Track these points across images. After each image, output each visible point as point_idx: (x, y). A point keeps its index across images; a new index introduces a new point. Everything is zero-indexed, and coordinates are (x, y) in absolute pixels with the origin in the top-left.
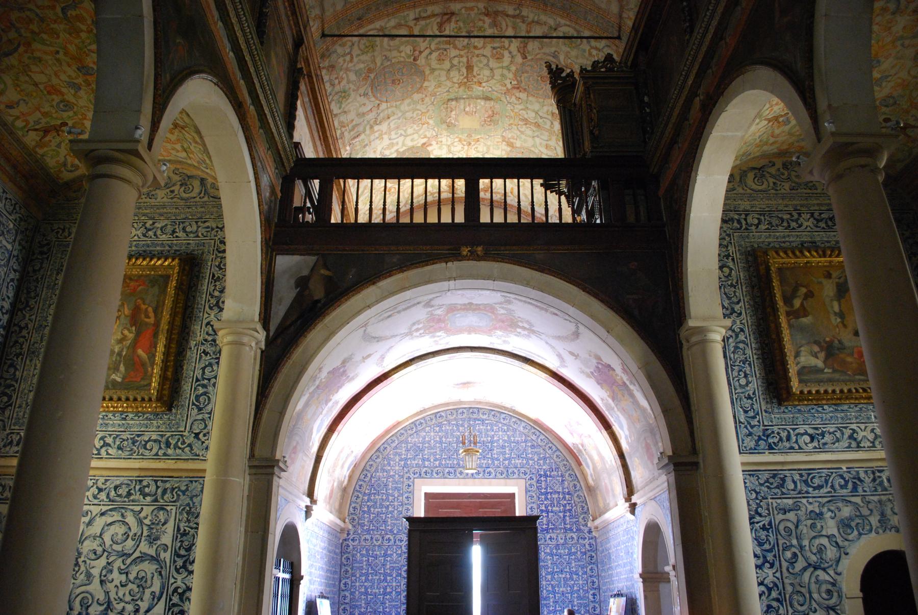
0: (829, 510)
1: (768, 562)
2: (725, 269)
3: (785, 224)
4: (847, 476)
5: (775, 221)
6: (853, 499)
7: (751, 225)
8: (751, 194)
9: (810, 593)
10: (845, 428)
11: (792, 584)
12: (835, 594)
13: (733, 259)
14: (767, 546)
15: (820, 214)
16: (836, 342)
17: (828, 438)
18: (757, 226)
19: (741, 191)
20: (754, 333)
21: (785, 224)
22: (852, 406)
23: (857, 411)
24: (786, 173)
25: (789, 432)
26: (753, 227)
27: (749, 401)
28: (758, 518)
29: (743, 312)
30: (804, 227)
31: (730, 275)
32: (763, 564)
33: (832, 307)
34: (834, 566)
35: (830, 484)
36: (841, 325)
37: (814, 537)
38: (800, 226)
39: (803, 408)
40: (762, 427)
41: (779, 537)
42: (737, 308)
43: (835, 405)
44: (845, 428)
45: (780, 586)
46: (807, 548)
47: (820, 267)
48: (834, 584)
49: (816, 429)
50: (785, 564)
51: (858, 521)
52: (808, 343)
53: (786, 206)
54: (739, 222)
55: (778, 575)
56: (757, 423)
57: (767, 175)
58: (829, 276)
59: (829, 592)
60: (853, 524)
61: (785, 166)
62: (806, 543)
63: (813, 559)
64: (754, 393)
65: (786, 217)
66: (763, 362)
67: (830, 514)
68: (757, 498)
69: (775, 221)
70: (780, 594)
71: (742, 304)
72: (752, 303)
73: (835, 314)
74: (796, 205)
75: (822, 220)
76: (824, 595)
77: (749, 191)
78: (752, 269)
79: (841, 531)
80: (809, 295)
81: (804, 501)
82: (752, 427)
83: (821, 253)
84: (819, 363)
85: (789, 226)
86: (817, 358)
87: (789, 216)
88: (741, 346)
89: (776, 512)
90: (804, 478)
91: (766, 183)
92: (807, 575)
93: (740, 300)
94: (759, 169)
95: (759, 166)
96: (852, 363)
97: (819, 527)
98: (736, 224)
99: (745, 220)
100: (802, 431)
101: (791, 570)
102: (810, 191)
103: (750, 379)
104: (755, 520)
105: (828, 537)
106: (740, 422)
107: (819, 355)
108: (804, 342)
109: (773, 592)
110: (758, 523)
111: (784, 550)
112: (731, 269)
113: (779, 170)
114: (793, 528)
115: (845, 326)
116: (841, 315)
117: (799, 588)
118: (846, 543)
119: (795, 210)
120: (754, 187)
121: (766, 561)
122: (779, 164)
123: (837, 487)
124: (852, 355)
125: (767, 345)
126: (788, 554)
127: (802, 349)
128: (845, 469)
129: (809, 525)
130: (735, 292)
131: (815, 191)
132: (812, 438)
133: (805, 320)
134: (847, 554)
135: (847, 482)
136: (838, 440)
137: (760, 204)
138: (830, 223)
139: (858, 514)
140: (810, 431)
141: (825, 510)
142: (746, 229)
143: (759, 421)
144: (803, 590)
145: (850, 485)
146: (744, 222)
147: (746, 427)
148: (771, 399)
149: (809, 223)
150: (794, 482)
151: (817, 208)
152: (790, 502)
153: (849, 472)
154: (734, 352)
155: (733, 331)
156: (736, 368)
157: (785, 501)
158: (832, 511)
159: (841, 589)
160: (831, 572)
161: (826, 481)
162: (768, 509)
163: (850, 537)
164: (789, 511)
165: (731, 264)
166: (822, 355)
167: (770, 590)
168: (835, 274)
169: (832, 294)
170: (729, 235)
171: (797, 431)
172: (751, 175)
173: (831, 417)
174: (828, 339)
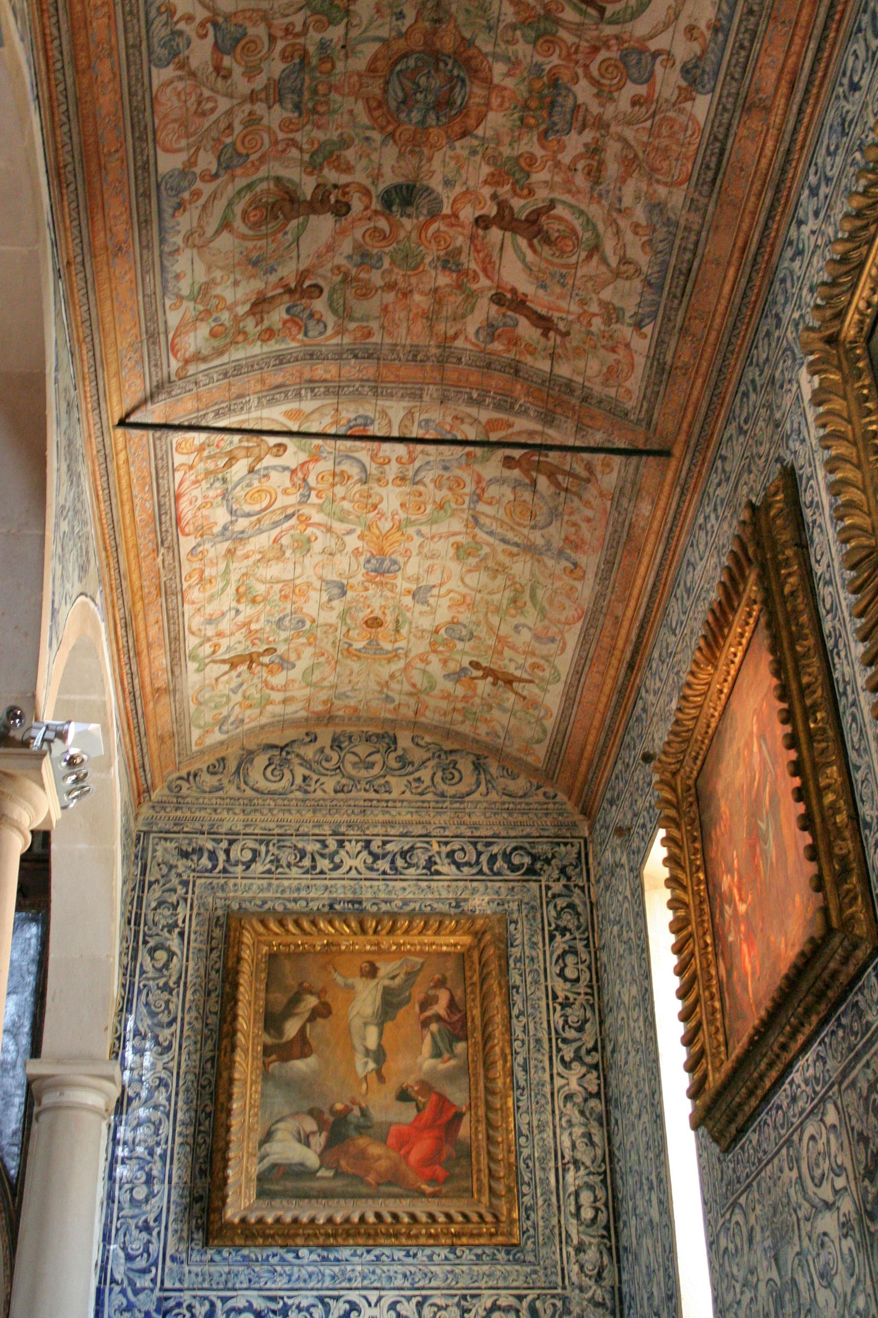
3: (307, 862)
5: (286, 856)
7: (236, 864)
8: (250, 800)
13: (181, 934)
15: (385, 843)
16: (356, 1112)
18: (248, 866)
19: (232, 791)
20: (187, 1090)
21: (307, 862)
24: (335, 757)
25: (212, 1305)
26: (240, 868)
27: (144, 1235)
29: (176, 1046)
30: (344, 869)
31: (166, 966)
33: (364, 1038)
36: (373, 1077)
38: (337, 867)
40: (157, 1293)
43: (324, 1247)
44: (337, 1298)
47: (360, 952)
52: (295, 1114)
53: (319, 825)
54: (213, 856)
56: (148, 1284)
57: (296, 761)
58: (372, 972)
61: (336, 743)
64: (157, 1219)
65: (312, 847)
66: (193, 1150)
69: (286, 856)
71: (177, 1027)
72: (198, 1025)
73: (367, 1052)
74: (339, 825)
75: (384, 856)
77: (249, 793)
78: (215, 954)
80: (322, 1011)
82: (136, 1292)
84: (312, 1159)
85: (314, 867)
86: (308, 1145)
87: (318, 846)
91: (288, 776)
93: (174, 1020)
94: (282, 749)
95: (282, 743)
96: (380, 1157)
98: (205, 862)
99: (227, 852)
100: (241, 1303)
102: (373, 795)
106: (113, 1281)
107: (313, 1140)
108: (286, 1111)
112: (171, 954)
113: (322, 750)
115: (381, 1078)
116: (379, 1055)
119: (335, 833)
120: (263, 784)
122: (325, 738)
124: (383, 1140)
125: (208, 1115)
127: (281, 1125)
130: (167, 1002)
131: (386, 796)
133: (301, 1065)
137: (266, 821)
138: (400, 863)
142: (225, 871)
143: (153, 1281)
146: (222, 857)
147: (123, 1292)
149: (358, 863)
151: (380, 830)
165: (174, 943)
166: (319, 1141)
168: (385, 969)
169: (369, 1011)
170: (185, 883)
171: (230, 1304)
172: (261, 760)
173: (310, 1275)
174: (339, 1106)
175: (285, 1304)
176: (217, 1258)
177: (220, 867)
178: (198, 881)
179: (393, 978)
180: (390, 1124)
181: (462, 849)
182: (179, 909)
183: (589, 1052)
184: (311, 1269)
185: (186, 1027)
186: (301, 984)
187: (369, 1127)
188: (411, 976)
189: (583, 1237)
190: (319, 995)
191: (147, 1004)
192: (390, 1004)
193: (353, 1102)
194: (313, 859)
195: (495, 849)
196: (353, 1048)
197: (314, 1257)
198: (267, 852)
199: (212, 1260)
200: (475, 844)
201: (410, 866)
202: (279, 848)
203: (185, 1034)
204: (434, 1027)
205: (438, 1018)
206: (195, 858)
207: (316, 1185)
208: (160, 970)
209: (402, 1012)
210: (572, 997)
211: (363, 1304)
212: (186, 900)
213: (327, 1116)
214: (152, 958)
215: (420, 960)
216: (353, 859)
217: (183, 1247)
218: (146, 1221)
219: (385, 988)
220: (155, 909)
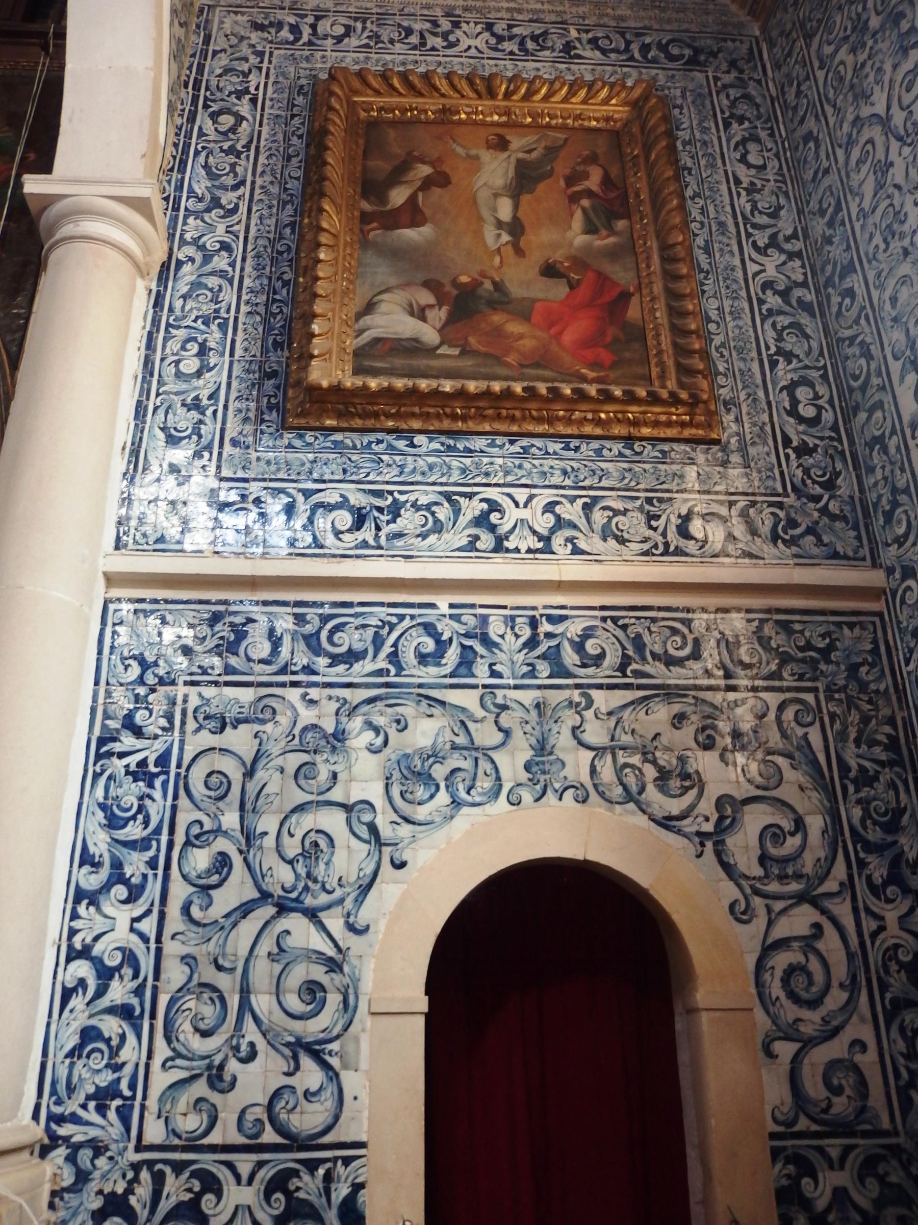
0: (369, 725)
1: (126, 882)
2: (222, 118)
4: (446, 629)
5: (386, 34)
6: (454, 697)
7: (325, 37)
9: (245, 991)
10: (470, 496)
11: (188, 960)
12: (334, 999)
14: (134, 831)
15: (510, 27)
16: (488, 285)
17: (409, 521)
18: (339, 39)
21: (414, 39)
22: (499, 440)
23: (514, 455)
27: (194, 415)
28: (128, 741)
32: (106, 887)
33: (494, 210)
34: (349, 904)
35: (387, 649)
36: (509, 251)
37: (300, 808)
39: (349, 439)
41: (183, 801)
42: (228, 198)
44: (470, 496)
45: (147, 964)
46: (269, 842)
48: (334, 965)
49: (378, 494)
50: (179, 891)
51: (456, 761)
54: (295, 29)
55: (148, 926)
58: (502, 144)
59: (313, 991)
60: (439, 772)
62: (268, 823)
63: (283, 876)
66: (265, 321)
67: (369, 735)
68: (141, 681)
70: (139, 992)
73: (500, 224)
74: (454, 8)
76: (294, 1003)
78: (296, 121)
79: (395, 791)
80: (439, 180)
81: (293, 695)
83: (481, 86)
84: (429, 334)
85: (423, 44)
86: (423, 319)
87: (428, 25)
88: (213, 282)
89: (191, 725)
90: (308, 629)
92: (248, 928)
93: (243, 183)
96: (521, 337)
97: (323, 774)
98: (285, 34)
99: (314, 27)
101: (196, 912)
103: (212, 362)
104: (117, 747)
105: (347, 808)
107: (430, 314)
109: (115, 984)
110: (121, 755)
111: (188, 843)
112: (240, 119)
114: (235, 773)
115: (519, 252)
116: (516, 228)
117: (208, 974)
118: (405, 830)
119: (447, 15)
121: (118, 876)
123: (409, 657)
126: (200, 859)
127: (384, 296)
128: (444, 608)
129: (291, 769)
130: (233, 166)
132: (359, 521)
133: (410, 234)
134: (400, 865)
135: (442, 646)
136: (438, 528)
138: (530, 45)
139: (461, 740)
140: (357, 499)
141: (357, 722)
142: (310, 43)
144: (224, 982)
145: (452, 655)
146: (306, 32)
148: (260, 411)
149: (479, 42)
150: (275, 642)
152: (246, 695)
153: (456, 618)
154: (184, 297)
155: (202, 248)
156: (181, 334)
157: (230, 692)
158: (377, 730)
159: (356, 981)
160: (334, 923)
161: (378, 642)
162: (169, 717)
163: (421, 813)
164: (237, 723)
165: (244, 108)
166: (440, 315)
167: (105, 974)
168: (517, 142)
169: (499, 182)
170: (261, 54)
173: (431, 467)
174: (464, 279)
175: (395, 501)
176: (297, 443)
177: (305, 38)
178: (276, 52)
179: (529, 152)
180: (534, 301)
181: (608, 37)
182: (251, 77)
183: (788, 239)
184: (431, 460)
185: (258, 191)
186: (409, 153)
187: (508, 303)
188: (552, 152)
189: (805, 438)
190: (432, 164)
191: (206, 166)
192: (525, 179)
193: (483, 274)
194: (422, 36)
195: (648, 40)
196: (480, 219)
197: (435, 445)
198: (364, 29)
199: (290, 446)
200: (623, 35)
201: (543, 48)
202: (379, 25)
203: (256, 197)
204: (585, 203)
205: (589, 193)
206: (273, 31)
207: (435, 363)
208: (225, 134)
209: (541, 187)
210: (759, 183)
211: (506, 503)
212: (260, 69)
213: (448, 288)
214: (215, 122)
215: (562, 136)
216: (472, 38)
217: (249, 428)
218: (197, 398)
219: (519, 161)
220: (220, 76)
